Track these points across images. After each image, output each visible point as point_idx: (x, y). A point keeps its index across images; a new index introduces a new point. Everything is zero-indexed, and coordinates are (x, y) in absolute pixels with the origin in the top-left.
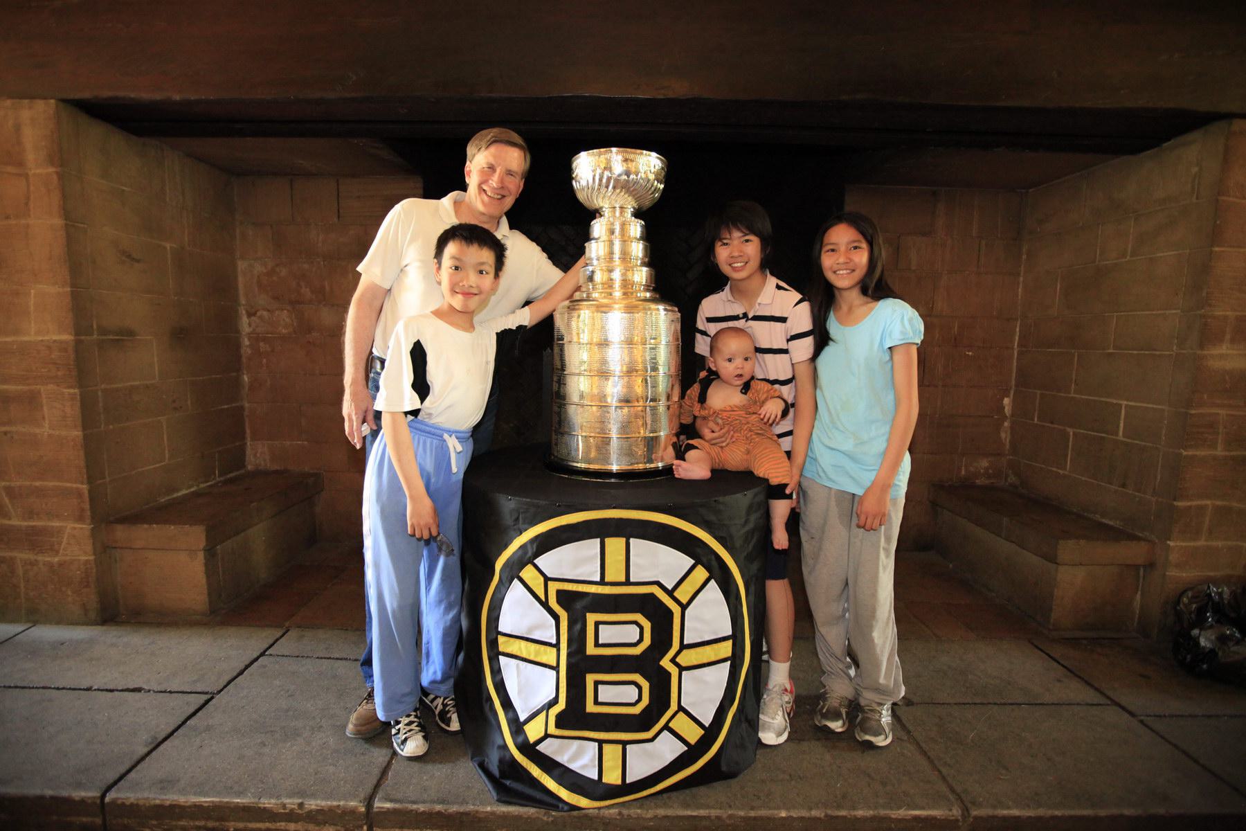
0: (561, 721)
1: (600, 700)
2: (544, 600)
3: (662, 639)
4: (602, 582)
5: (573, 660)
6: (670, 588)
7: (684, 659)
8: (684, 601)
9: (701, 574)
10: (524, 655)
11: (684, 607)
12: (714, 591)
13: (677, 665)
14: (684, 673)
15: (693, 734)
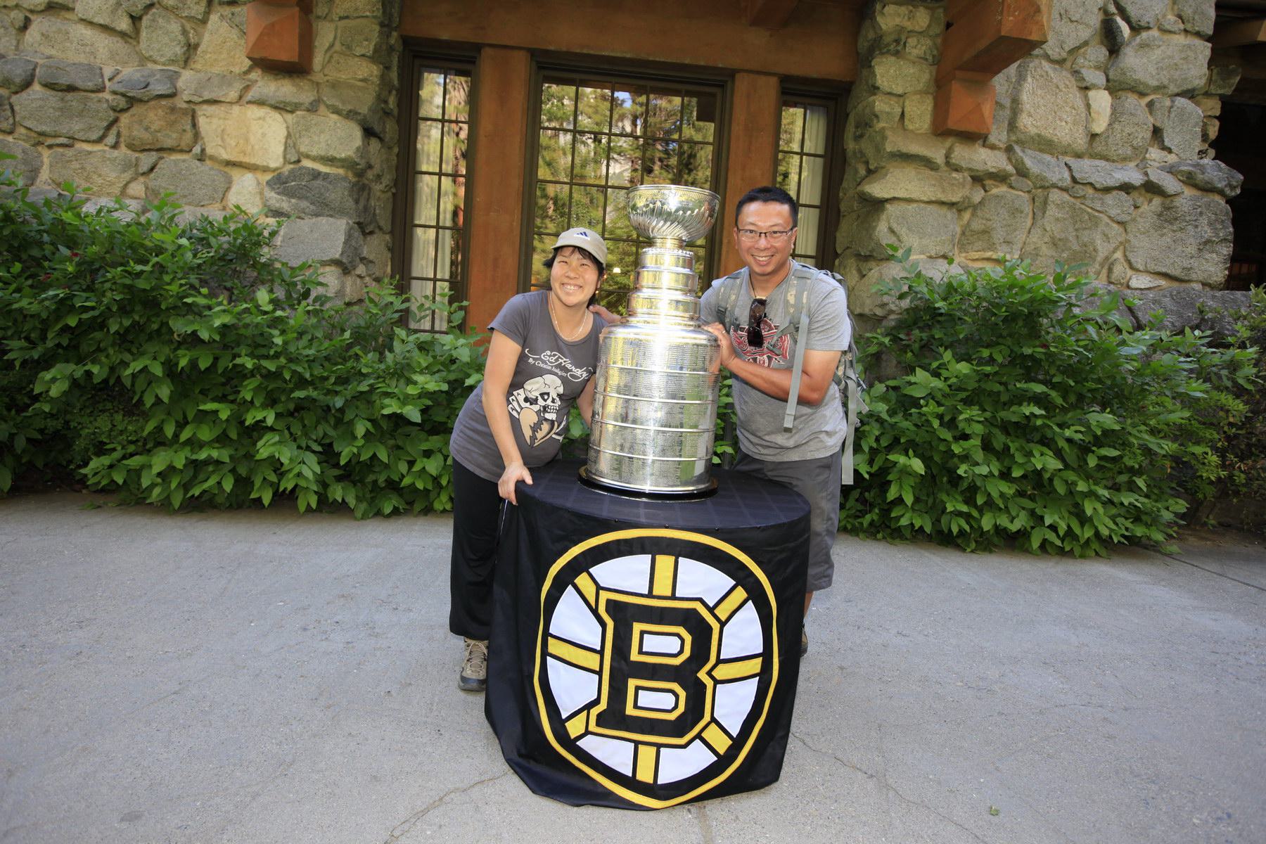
0: (602, 720)
1: (639, 704)
2: (593, 605)
3: (701, 652)
4: (650, 595)
5: (615, 664)
6: (711, 605)
7: (721, 672)
8: (723, 619)
9: (740, 594)
10: (568, 659)
11: (723, 624)
12: (750, 611)
13: (713, 678)
14: (718, 686)
15: (722, 744)
